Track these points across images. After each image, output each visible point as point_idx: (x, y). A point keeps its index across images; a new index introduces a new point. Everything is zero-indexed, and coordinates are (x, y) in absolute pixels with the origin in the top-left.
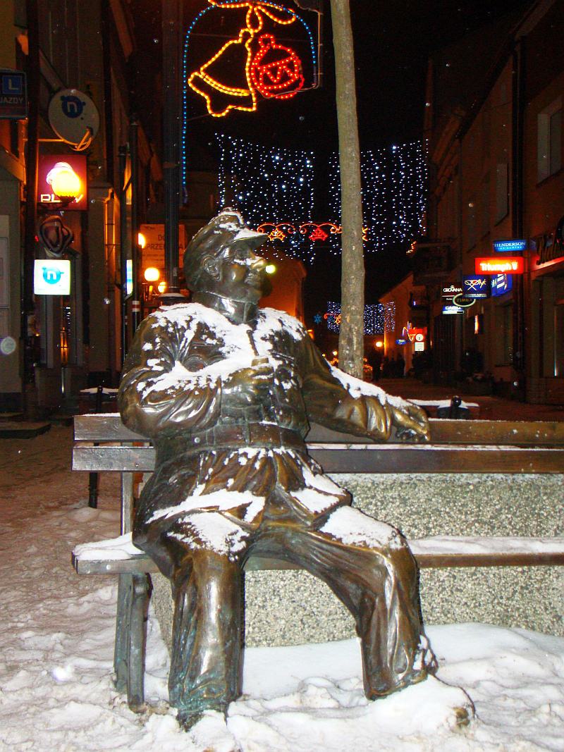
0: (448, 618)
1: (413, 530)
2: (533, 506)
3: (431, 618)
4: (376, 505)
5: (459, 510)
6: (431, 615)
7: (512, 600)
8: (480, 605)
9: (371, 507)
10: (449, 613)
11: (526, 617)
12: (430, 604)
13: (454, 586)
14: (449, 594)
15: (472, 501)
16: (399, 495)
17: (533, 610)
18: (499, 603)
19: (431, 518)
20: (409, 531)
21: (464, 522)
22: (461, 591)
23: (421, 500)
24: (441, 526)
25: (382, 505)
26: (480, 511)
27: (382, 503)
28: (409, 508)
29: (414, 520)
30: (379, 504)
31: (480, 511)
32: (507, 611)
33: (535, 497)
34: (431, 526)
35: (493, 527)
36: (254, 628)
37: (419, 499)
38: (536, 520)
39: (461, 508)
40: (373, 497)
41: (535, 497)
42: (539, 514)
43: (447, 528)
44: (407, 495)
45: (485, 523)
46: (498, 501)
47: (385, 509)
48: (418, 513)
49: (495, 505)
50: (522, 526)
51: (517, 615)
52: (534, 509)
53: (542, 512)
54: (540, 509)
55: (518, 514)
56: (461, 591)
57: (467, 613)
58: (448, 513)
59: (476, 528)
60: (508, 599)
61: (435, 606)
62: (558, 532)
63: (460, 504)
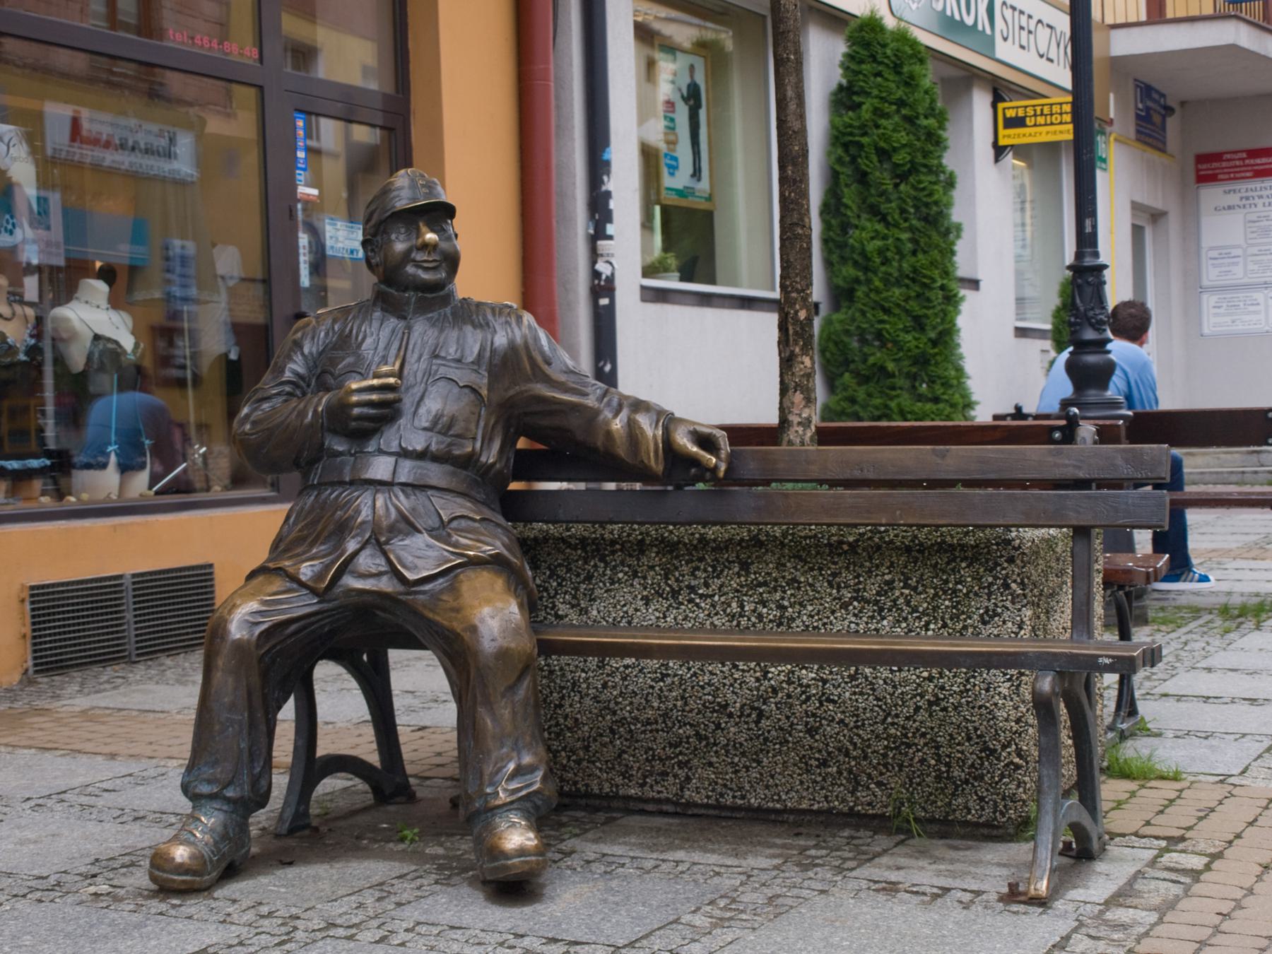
0: (817, 741)
1: (760, 608)
2: (944, 577)
3: (790, 739)
4: (705, 571)
5: (828, 581)
7: (915, 721)
8: (863, 725)
9: (698, 573)
11: (937, 748)
12: (788, 718)
13: (823, 694)
15: (847, 568)
16: (738, 557)
17: (948, 738)
18: (893, 724)
19: (784, 592)
20: (754, 611)
21: (835, 599)
22: (834, 702)
23: (771, 566)
24: (801, 604)
25: (713, 572)
26: (860, 583)
27: (714, 567)
28: (753, 576)
29: (761, 594)
30: (710, 569)
32: (905, 736)
33: (948, 563)
34: (786, 603)
35: (881, 610)
36: (550, 734)
37: (767, 564)
38: (950, 600)
39: (831, 578)
40: (701, 559)
41: (948, 563)
42: (955, 591)
43: (810, 608)
44: (749, 557)
45: (868, 602)
46: (888, 568)
47: (718, 577)
48: (765, 584)
49: (884, 574)
50: (928, 608)
51: (922, 743)
52: (946, 582)
53: (960, 587)
54: (957, 583)
55: (920, 589)
56: (834, 702)
57: (844, 736)
59: (855, 608)
60: (908, 718)
61: (795, 721)
63: (829, 572)
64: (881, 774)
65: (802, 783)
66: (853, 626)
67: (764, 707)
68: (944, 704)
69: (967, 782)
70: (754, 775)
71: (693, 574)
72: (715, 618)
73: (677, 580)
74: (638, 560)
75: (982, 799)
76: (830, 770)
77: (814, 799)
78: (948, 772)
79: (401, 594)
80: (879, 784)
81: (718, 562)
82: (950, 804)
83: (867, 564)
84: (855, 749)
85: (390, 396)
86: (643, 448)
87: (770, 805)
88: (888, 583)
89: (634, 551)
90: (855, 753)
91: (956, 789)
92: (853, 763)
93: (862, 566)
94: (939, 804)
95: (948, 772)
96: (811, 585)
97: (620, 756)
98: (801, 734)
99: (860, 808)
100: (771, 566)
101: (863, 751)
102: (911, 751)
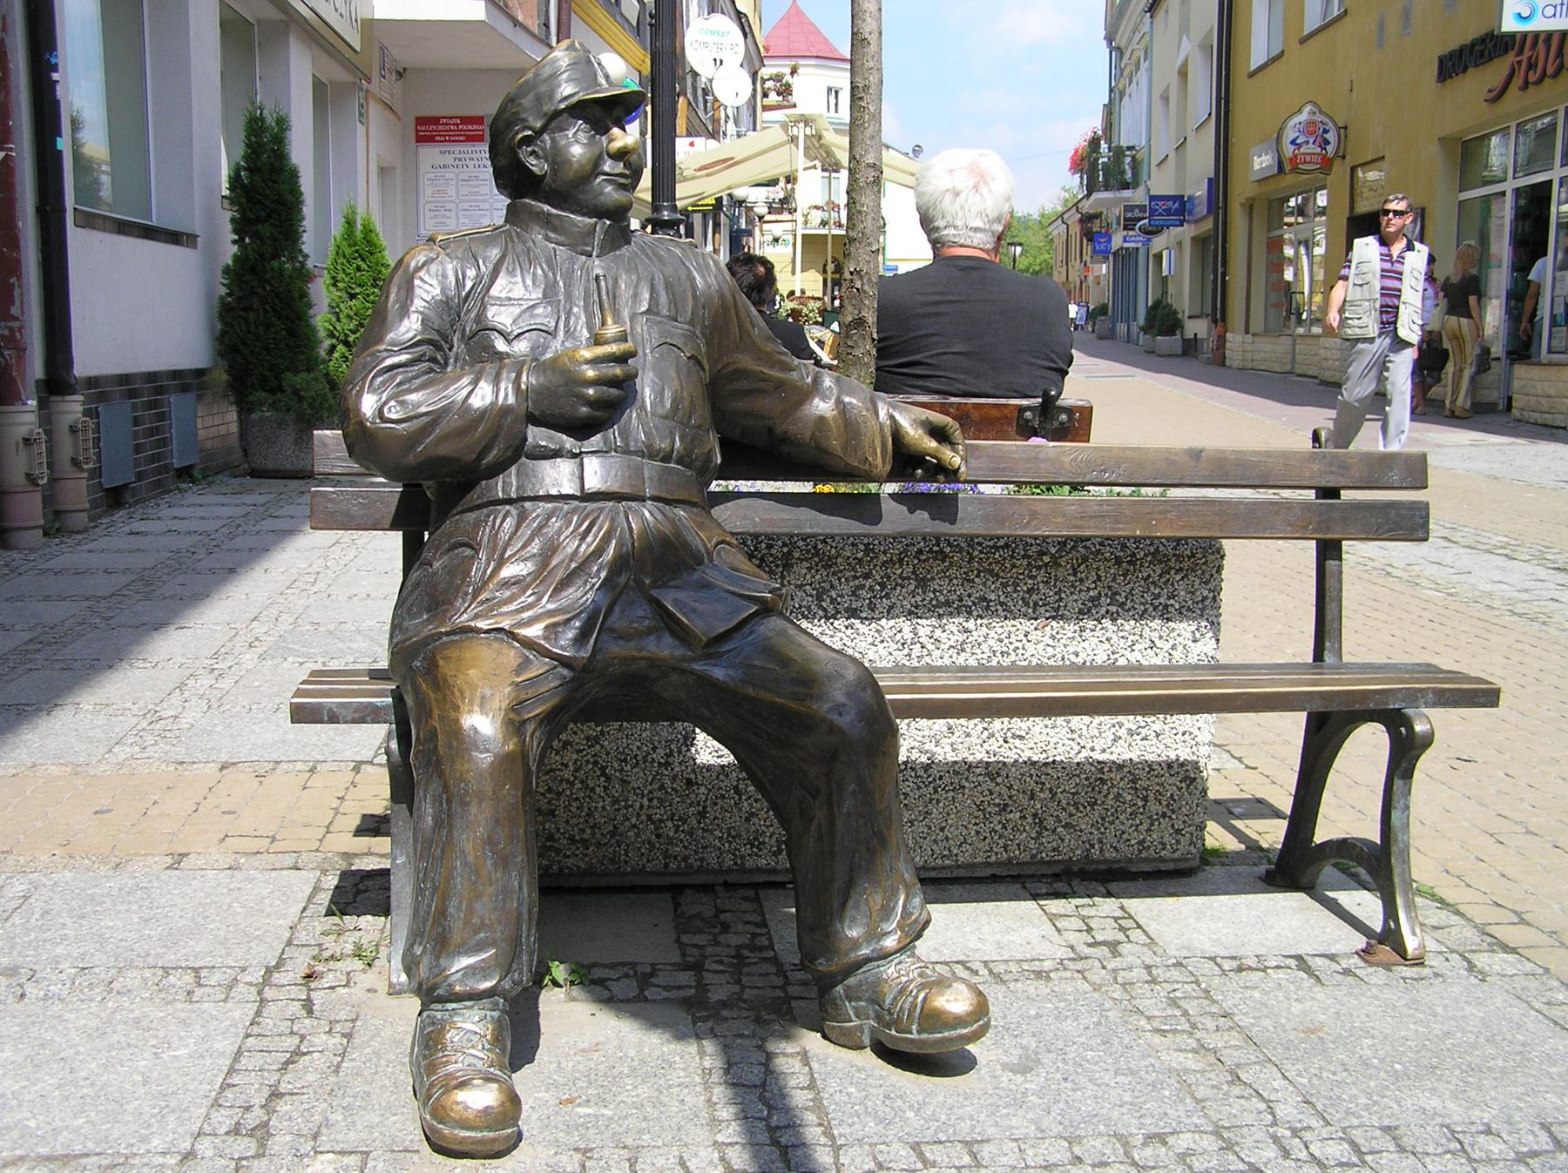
0: (998, 784)
3: (967, 785)
4: (871, 589)
5: (1023, 599)
6: (967, 779)
9: (863, 593)
10: (999, 775)
11: (1134, 781)
14: (1001, 742)
22: (1021, 738)
23: (955, 582)
27: (882, 585)
30: (878, 587)
31: (1061, 599)
33: (1160, 576)
36: (650, 800)
40: (866, 576)
44: (929, 572)
47: (887, 596)
49: (1089, 589)
54: (1169, 598)
55: (1129, 605)
56: (1021, 738)
57: (1031, 776)
58: (1002, 604)
62: (1198, 635)
64: (1071, 815)
65: (978, 833)
66: (1049, 649)
67: (935, 750)
68: (1144, 732)
69: (1164, 815)
70: (921, 829)
71: (854, 594)
72: (881, 646)
73: (833, 601)
74: (783, 577)
75: (1178, 831)
76: (1012, 816)
77: (991, 850)
78: (1144, 807)
79: (684, 659)
80: (1067, 826)
81: (889, 578)
82: (1144, 841)
83: (1071, 578)
84: (1042, 790)
85: (618, 371)
86: (866, 442)
87: (939, 862)
88: (1092, 599)
89: (777, 566)
90: (1042, 795)
91: (1152, 824)
92: (1039, 806)
93: (1065, 580)
94: (1133, 842)
95: (1144, 807)
96: (1002, 604)
97: (748, 820)
98: (980, 778)
99: (1044, 855)
100: (955, 582)
101: (1051, 790)
102: (1106, 787)
